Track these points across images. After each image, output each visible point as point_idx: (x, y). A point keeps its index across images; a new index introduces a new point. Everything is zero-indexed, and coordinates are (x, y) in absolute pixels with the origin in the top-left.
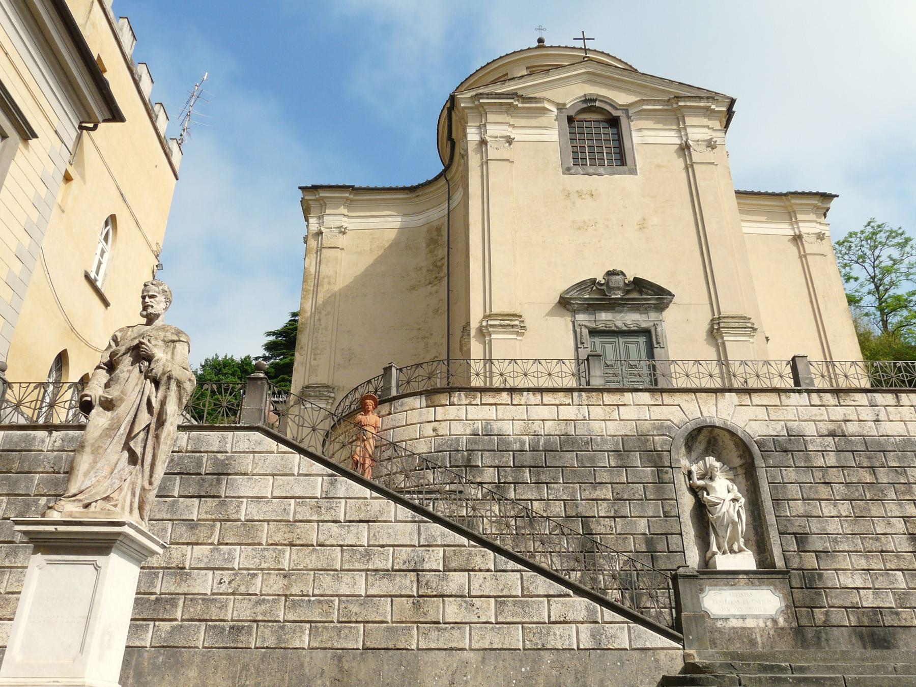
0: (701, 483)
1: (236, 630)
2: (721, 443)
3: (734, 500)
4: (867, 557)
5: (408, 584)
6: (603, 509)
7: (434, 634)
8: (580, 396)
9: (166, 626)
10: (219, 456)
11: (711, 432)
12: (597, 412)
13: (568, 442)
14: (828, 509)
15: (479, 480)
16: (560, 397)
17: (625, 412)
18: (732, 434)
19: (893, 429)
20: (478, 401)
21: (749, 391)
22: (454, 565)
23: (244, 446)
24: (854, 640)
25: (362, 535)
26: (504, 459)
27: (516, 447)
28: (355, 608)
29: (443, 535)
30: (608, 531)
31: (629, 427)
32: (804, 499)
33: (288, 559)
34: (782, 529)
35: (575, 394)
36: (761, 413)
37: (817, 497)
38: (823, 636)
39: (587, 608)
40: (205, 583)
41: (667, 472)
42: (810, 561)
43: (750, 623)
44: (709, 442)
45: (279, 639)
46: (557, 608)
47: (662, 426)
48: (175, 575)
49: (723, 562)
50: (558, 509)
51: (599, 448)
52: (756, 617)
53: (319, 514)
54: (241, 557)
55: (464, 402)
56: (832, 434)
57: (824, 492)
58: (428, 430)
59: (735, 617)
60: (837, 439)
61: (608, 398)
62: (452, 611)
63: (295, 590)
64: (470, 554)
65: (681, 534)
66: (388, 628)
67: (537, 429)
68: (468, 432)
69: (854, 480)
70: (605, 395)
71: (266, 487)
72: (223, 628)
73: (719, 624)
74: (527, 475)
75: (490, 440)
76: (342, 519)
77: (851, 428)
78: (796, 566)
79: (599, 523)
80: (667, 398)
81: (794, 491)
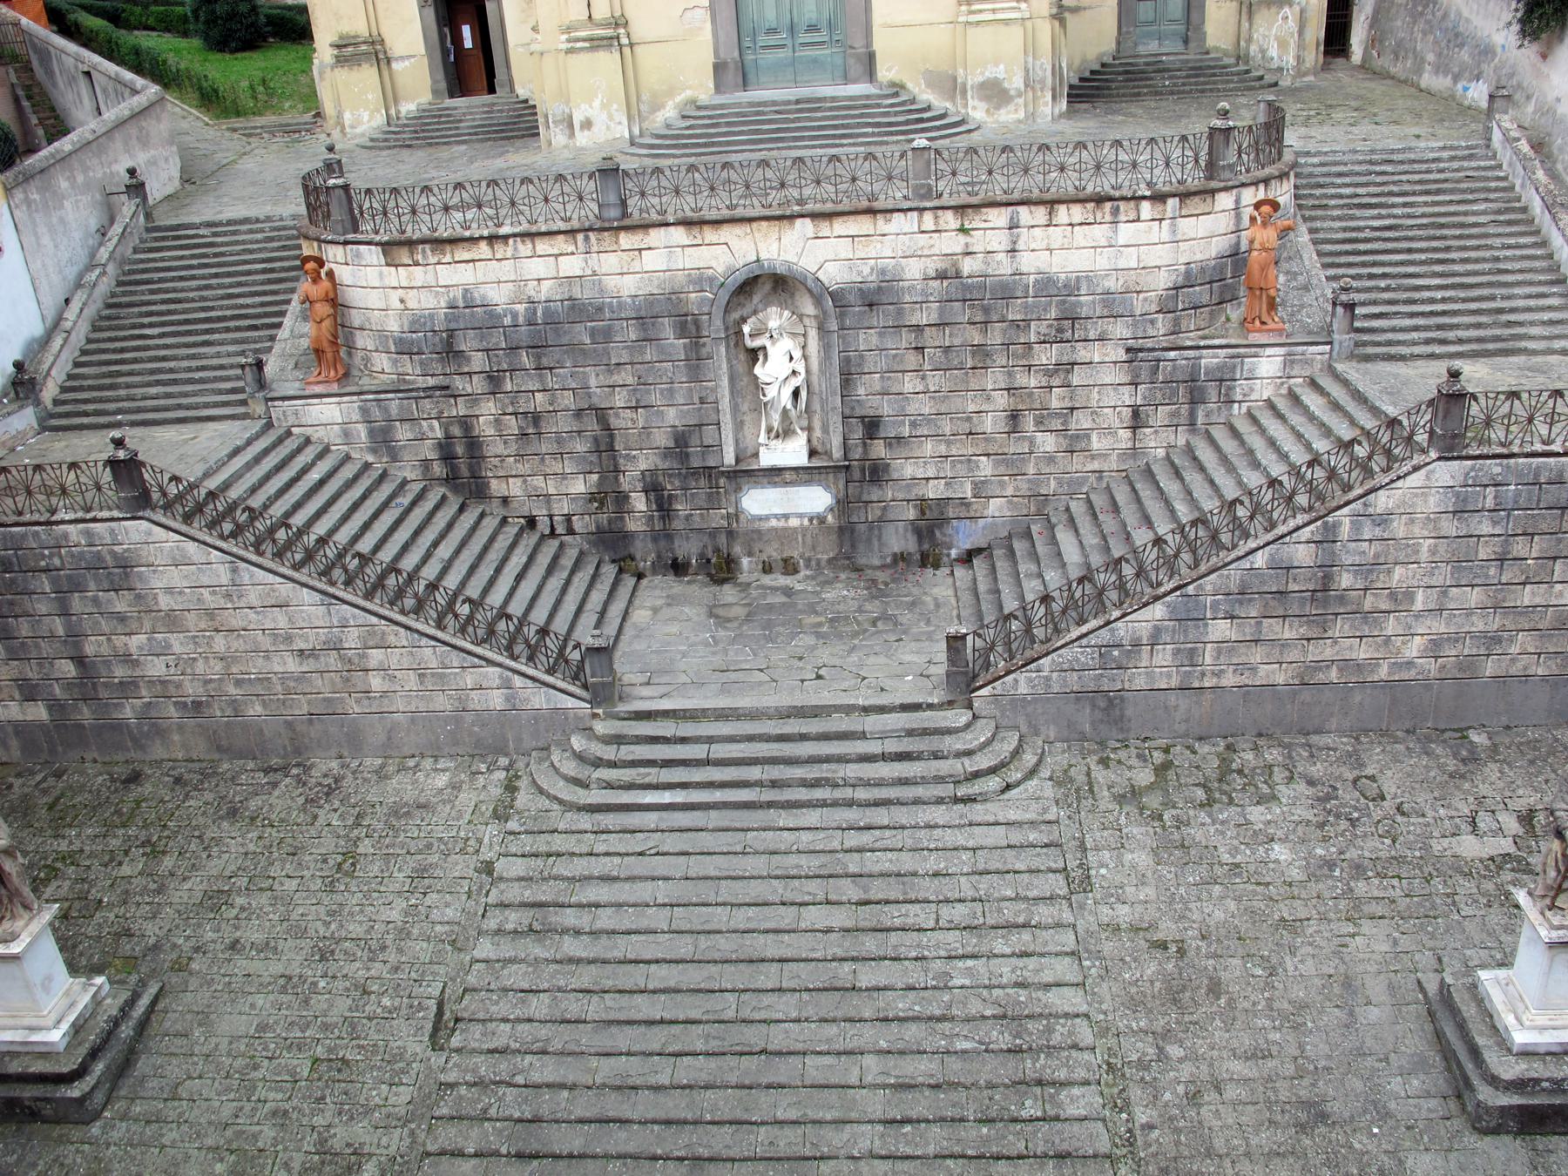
1: (197, 705)
4: (948, 443)
5: (331, 661)
6: (620, 399)
7: (366, 702)
8: (587, 239)
10: (116, 548)
12: (610, 262)
13: (577, 310)
14: (910, 384)
16: (561, 244)
17: (652, 261)
19: (1030, 263)
20: (448, 258)
21: (830, 216)
22: (371, 643)
23: (135, 537)
24: (909, 535)
25: (280, 620)
26: (494, 340)
27: (507, 321)
28: (292, 684)
29: (354, 617)
30: (630, 425)
31: (656, 282)
34: (847, 412)
35: (580, 237)
36: (844, 248)
39: (501, 677)
40: (156, 668)
41: (704, 345)
42: (879, 450)
43: (794, 522)
46: (469, 679)
48: (126, 661)
49: (767, 459)
50: (567, 400)
51: (615, 316)
52: (801, 516)
53: (232, 601)
54: (177, 643)
55: (433, 260)
56: (942, 276)
57: (912, 360)
58: (394, 297)
59: (776, 516)
60: (945, 283)
61: (626, 240)
62: (376, 682)
64: (384, 633)
66: (325, 699)
67: (532, 293)
68: (443, 304)
69: (957, 342)
70: (622, 235)
71: (175, 577)
72: (185, 704)
73: (756, 525)
74: (525, 360)
76: (255, 603)
77: (968, 266)
79: (617, 415)
80: (710, 235)
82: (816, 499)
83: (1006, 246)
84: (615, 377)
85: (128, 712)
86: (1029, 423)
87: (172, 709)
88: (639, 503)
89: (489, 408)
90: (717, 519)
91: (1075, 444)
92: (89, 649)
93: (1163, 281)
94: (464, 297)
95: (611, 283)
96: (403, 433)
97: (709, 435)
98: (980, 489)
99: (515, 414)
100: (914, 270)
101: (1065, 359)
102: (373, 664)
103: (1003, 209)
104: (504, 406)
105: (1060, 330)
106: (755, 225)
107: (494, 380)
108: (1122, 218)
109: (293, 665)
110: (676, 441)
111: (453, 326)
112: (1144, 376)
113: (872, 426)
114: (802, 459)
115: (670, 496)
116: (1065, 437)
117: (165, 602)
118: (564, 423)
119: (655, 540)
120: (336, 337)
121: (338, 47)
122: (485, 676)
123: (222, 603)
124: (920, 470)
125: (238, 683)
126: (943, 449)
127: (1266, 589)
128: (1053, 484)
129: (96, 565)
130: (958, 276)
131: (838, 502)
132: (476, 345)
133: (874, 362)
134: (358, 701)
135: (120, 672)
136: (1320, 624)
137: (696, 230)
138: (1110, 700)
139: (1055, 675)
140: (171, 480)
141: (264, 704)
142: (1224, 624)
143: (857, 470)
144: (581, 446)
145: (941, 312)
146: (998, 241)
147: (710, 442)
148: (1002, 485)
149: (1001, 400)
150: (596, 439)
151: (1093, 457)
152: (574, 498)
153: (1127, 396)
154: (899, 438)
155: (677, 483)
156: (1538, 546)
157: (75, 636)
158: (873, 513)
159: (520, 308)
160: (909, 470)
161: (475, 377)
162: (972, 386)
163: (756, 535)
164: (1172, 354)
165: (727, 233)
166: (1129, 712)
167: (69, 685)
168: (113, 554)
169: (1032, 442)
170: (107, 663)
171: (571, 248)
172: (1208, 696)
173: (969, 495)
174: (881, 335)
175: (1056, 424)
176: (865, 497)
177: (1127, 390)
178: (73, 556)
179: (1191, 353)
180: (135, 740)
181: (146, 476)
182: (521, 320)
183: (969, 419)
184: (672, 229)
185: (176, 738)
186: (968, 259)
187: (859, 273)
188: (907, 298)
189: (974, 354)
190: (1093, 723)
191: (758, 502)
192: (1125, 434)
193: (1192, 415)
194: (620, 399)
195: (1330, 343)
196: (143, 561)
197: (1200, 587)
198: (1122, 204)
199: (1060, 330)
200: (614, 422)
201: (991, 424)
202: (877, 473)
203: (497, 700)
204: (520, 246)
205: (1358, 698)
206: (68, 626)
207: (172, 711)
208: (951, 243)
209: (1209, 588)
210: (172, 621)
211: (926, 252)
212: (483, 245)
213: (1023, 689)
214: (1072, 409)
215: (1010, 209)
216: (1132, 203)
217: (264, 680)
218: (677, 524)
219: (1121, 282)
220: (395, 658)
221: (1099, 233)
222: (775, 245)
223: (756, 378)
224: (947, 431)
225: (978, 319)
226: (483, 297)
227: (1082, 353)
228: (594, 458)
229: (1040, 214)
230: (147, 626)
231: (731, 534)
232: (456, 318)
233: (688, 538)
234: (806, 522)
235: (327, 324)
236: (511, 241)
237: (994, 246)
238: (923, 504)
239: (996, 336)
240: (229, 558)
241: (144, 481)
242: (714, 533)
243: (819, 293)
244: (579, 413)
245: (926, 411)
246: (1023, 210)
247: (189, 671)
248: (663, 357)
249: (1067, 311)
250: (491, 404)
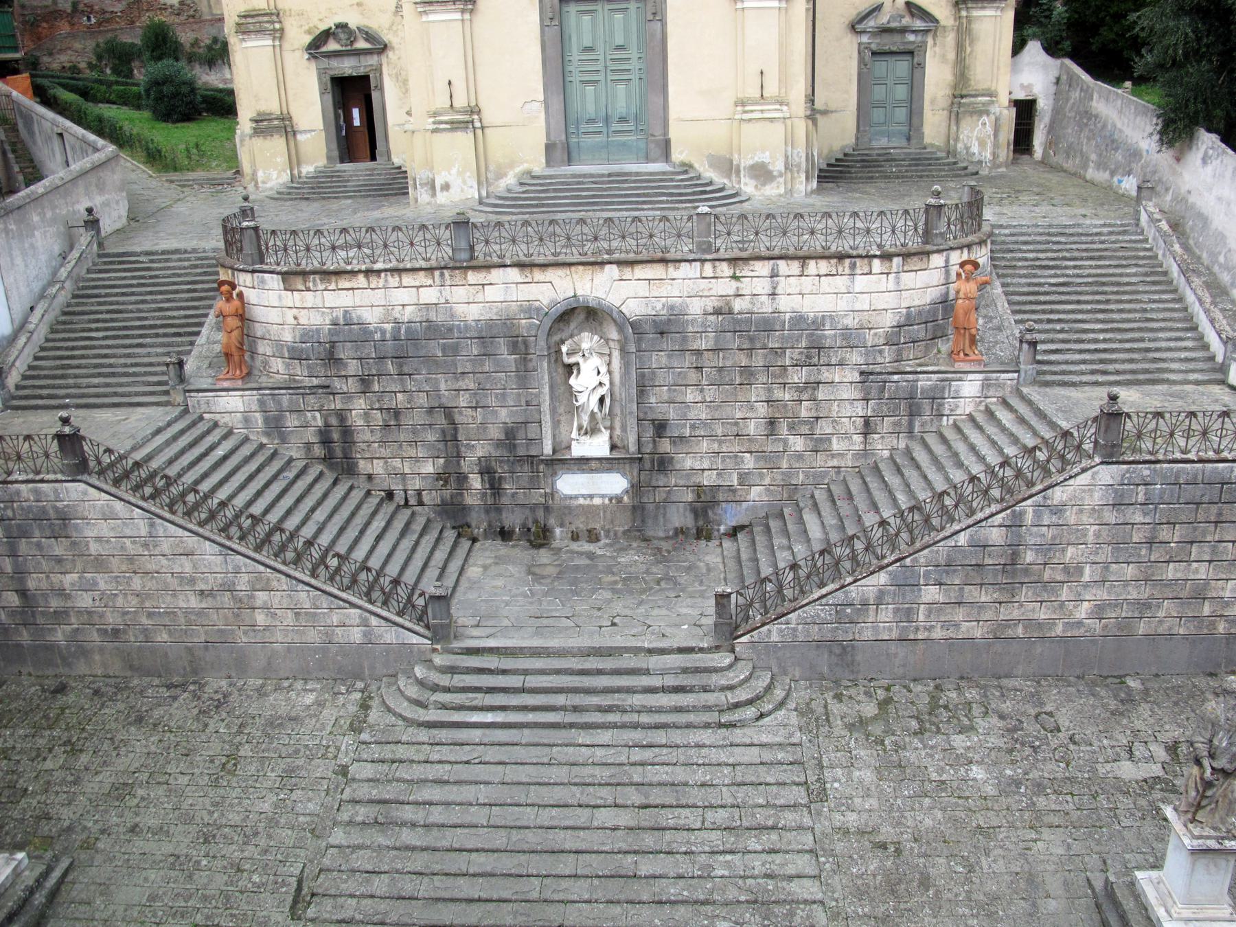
0: (572, 360)
1: (116, 632)
4: (720, 442)
5: (226, 599)
6: (463, 400)
7: (252, 634)
8: (442, 275)
9: (68, 628)
10: (58, 504)
13: (432, 330)
14: (691, 395)
15: (343, 373)
16: (422, 278)
17: (492, 294)
19: (786, 304)
20: (333, 286)
22: (258, 587)
23: (74, 496)
24: (688, 513)
25: (186, 566)
26: (366, 351)
27: (377, 336)
28: (193, 617)
29: (246, 565)
30: (470, 420)
33: (137, 583)
35: (437, 273)
36: (642, 289)
39: (360, 617)
40: (84, 601)
41: (531, 360)
42: (665, 446)
43: (597, 501)
45: (146, 636)
49: (578, 451)
50: (422, 399)
52: (603, 496)
53: (149, 550)
54: (103, 582)
55: (321, 287)
56: (717, 312)
57: (693, 376)
58: (290, 314)
59: (583, 496)
60: (720, 318)
61: (472, 277)
62: (260, 618)
63: (147, 604)
64: (268, 579)
67: (398, 316)
69: (728, 363)
70: (470, 273)
71: (104, 528)
72: (106, 631)
74: (390, 367)
75: (350, 331)
76: (167, 552)
77: (738, 305)
79: (461, 413)
80: (538, 275)
82: (615, 484)
83: (768, 290)
84: (460, 383)
85: (59, 636)
86: (783, 428)
87: (95, 634)
88: (476, 482)
89: (360, 404)
90: (537, 497)
91: (819, 445)
92: (31, 584)
93: (889, 320)
94: (344, 316)
95: (460, 310)
96: (291, 421)
97: (532, 431)
98: (744, 478)
99: (381, 409)
100: (696, 307)
101: (812, 379)
102: (259, 603)
103: (766, 262)
104: (372, 403)
105: (809, 357)
106: (573, 268)
107: (365, 382)
108: (858, 271)
109: (194, 602)
110: (507, 434)
111: (335, 339)
112: (874, 393)
113: (661, 427)
114: (604, 452)
115: (500, 478)
116: (812, 439)
117: (94, 548)
118: (418, 418)
119: (487, 512)
120: (242, 344)
121: (256, 121)
122: (348, 616)
123: (140, 551)
124: (698, 463)
125: (150, 615)
126: (715, 447)
127: (967, 562)
128: (801, 476)
129: (41, 517)
130: (730, 312)
131: (632, 486)
132: (352, 355)
133: (663, 377)
134: (245, 633)
135: (55, 603)
136: (1010, 590)
137: (527, 271)
138: (844, 648)
139: (800, 627)
140: (105, 451)
141: (170, 633)
142: (933, 590)
143: (648, 461)
144: (431, 437)
145: (717, 340)
146: (762, 286)
147: (533, 436)
148: (762, 476)
149: (762, 409)
150: (443, 431)
151: (833, 456)
152: (424, 477)
153: (859, 409)
154: (681, 437)
155: (506, 468)
156: (1179, 533)
157: (20, 573)
158: (660, 496)
159: (388, 327)
160: (689, 463)
161: (350, 380)
162: (740, 398)
163: (567, 510)
164: (896, 377)
165: (552, 274)
166: (859, 658)
167: (12, 613)
168: (55, 507)
169: (785, 442)
170: (45, 596)
171: (430, 282)
172: (921, 646)
173: (736, 483)
174: (669, 356)
175: (805, 429)
176: (654, 483)
177: (859, 404)
178: (22, 509)
179: (910, 377)
180: (64, 659)
181: (86, 448)
182: (388, 336)
183: (736, 424)
184: (509, 269)
185: (97, 657)
186: (738, 299)
188: (691, 329)
189: (741, 374)
190: (830, 666)
191: (569, 484)
192: (858, 439)
193: (911, 424)
194: (463, 400)
195: (1018, 371)
196: (79, 515)
197: (916, 560)
198: (858, 261)
199: (809, 357)
200: (458, 419)
201: (752, 428)
202: (663, 464)
203: (356, 635)
204: (389, 278)
205: (1039, 650)
206: (16, 565)
207: (95, 636)
208: (726, 287)
209: (922, 560)
210: (100, 564)
211: (706, 293)
212: (361, 277)
213: (775, 637)
214: (817, 418)
215: (772, 262)
216: (866, 261)
217: (170, 614)
218: (505, 500)
219: (856, 321)
220: (276, 599)
221: (841, 282)
222: (589, 285)
223: (571, 387)
224: (720, 432)
225: (745, 346)
226: (359, 317)
227: (826, 375)
228: (441, 446)
229: (795, 266)
230: (79, 567)
231: (547, 509)
232: (337, 333)
233: (513, 512)
234: (607, 501)
235: (236, 333)
236: (383, 275)
237: (759, 290)
238: (699, 489)
239: (758, 360)
240: (148, 515)
241: (83, 452)
242: (533, 508)
243: (621, 322)
244: (431, 410)
245: (703, 416)
246: (782, 263)
247: (111, 604)
249: (814, 341)
250: (362, 401)
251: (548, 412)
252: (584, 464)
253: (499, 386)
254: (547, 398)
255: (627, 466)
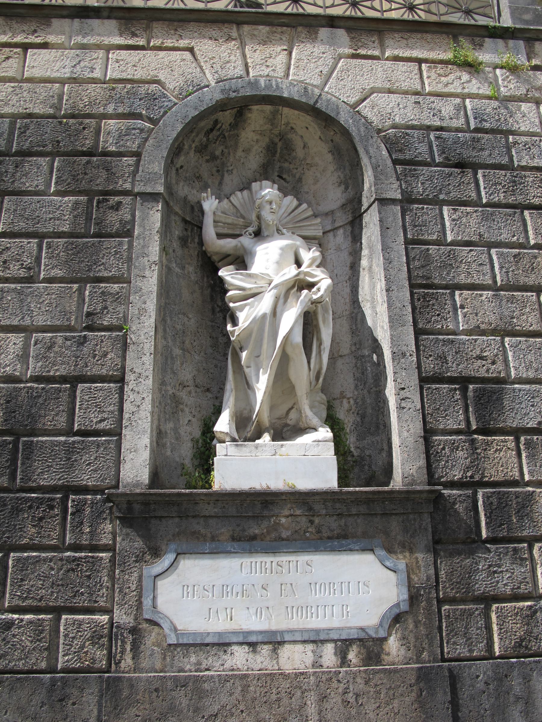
0: (228, 244)
2: (300, 153)
3: (302, 285)
11: (272, 119)
18: (322, 117)
32: (494, 287)
34: (430, 366)
37: (531, 280)
38: (516, 684)
41: (117, 207)
43: (295, 658)
44: (271, 149)
47: (132, 94)
49: (239, 468)
52: (316, 639)
65: (121, 380)
73: (189, 662)
78: (457, 475)
81: (471, 266)
82: (357, 589)
90: (75, 640)
97: (90, 407)
106: (246, 28)
113: (486, 396)
131: (414, 598)
174: (485, 218)
176: (482, 584)
187: (437, 113)
191: (202, 596)
222: (282, 58)
248: (21, 226)
251: (149, 346)
252: (260, 522)
253: (15, 270)
254: (151, 306)
255: (395, 525)
